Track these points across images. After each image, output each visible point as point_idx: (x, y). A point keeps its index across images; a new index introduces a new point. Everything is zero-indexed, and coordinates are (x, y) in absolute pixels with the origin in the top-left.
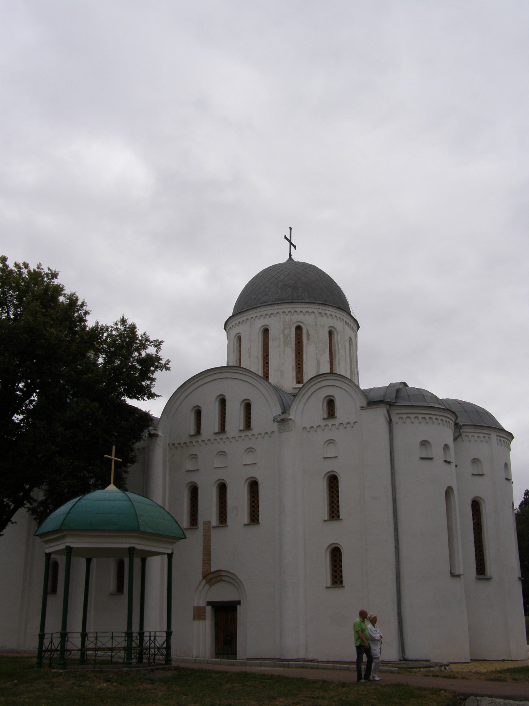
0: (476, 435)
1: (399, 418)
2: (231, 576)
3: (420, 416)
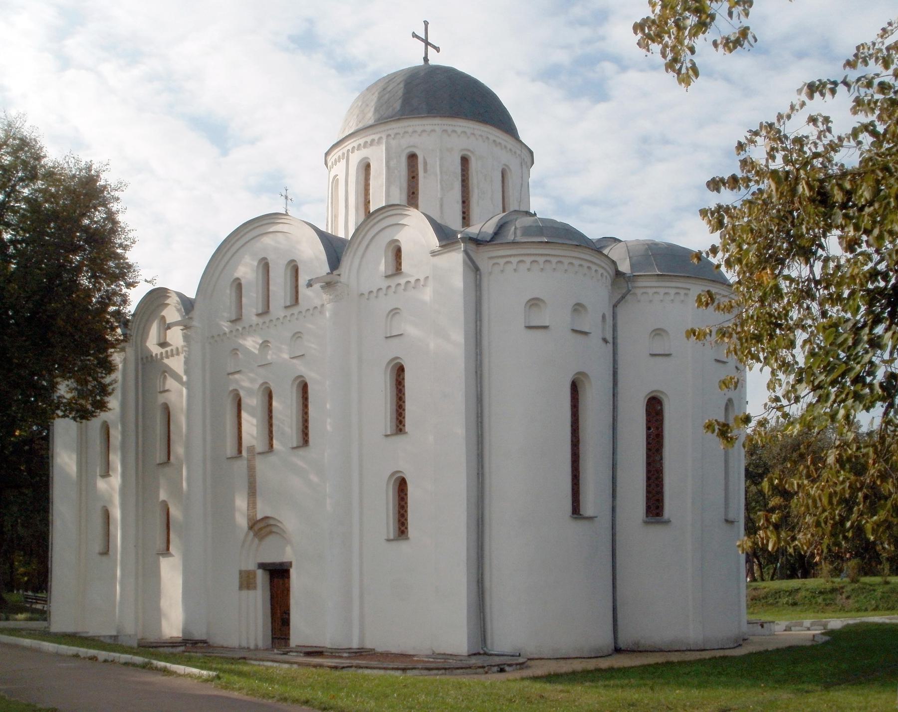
0: (662, 291)
1: (494, 264)
3: (528, 260)
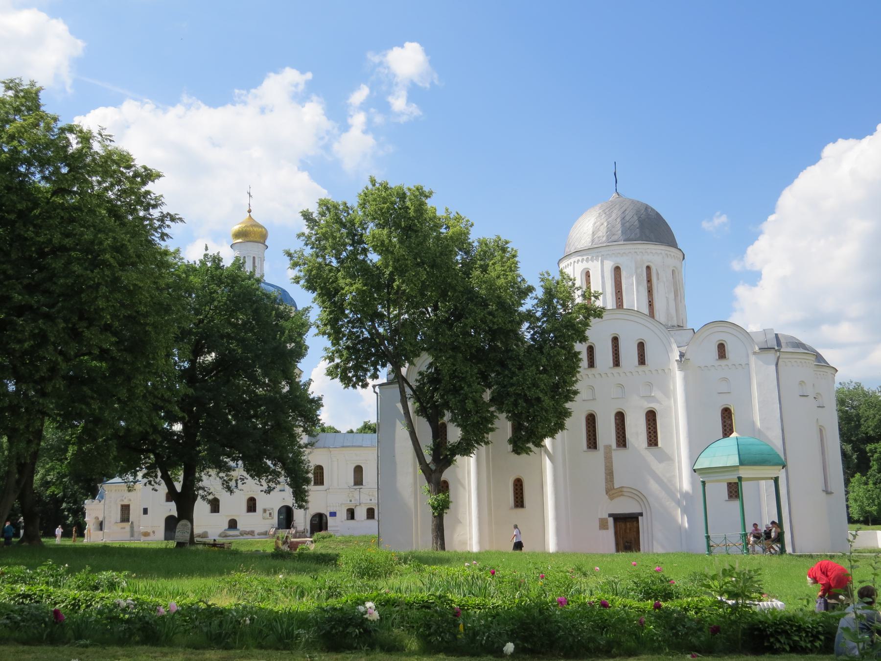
3: (799, 361)
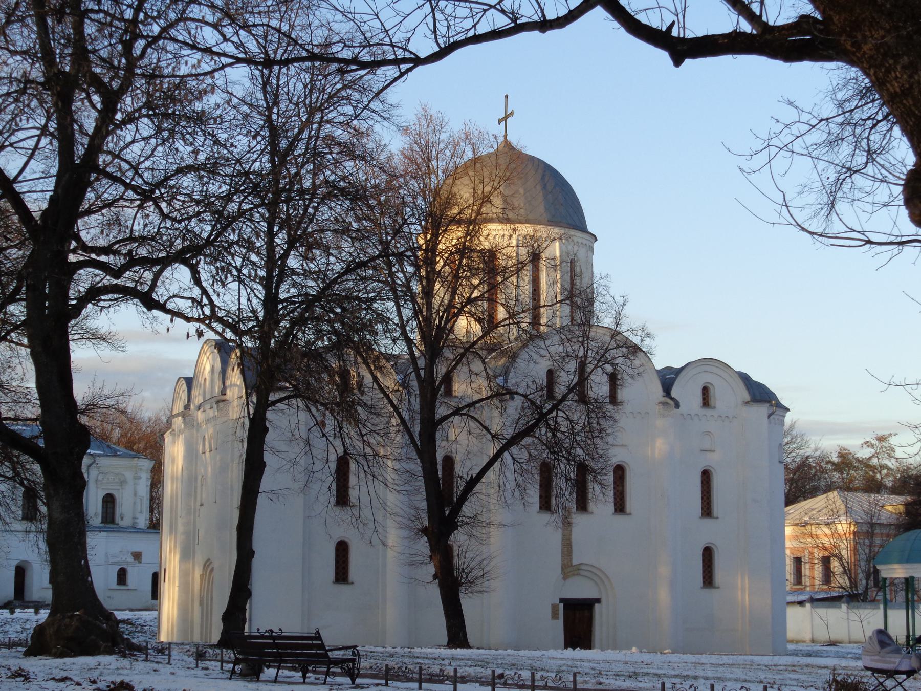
2: (594, 570)
